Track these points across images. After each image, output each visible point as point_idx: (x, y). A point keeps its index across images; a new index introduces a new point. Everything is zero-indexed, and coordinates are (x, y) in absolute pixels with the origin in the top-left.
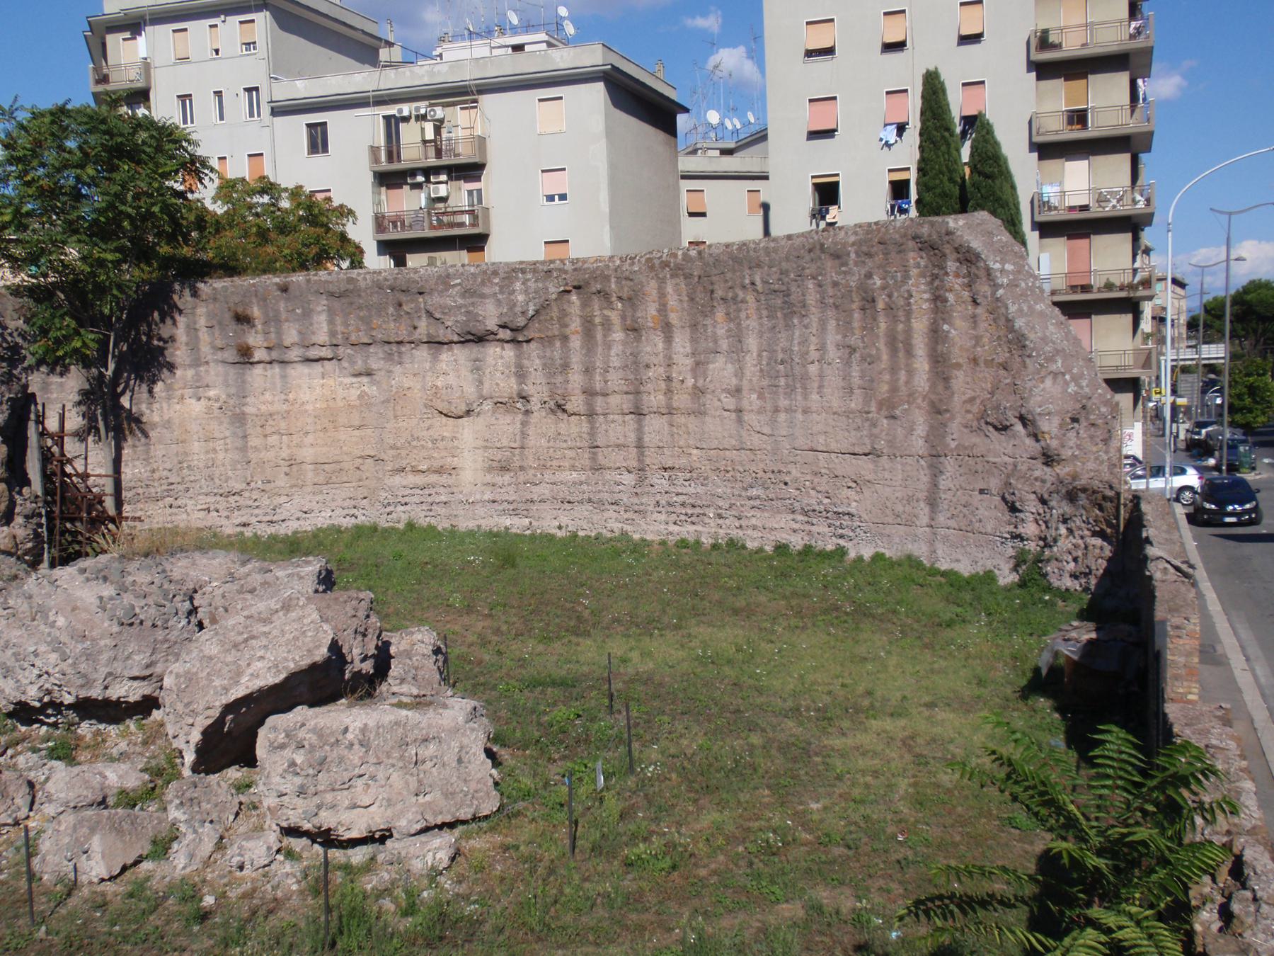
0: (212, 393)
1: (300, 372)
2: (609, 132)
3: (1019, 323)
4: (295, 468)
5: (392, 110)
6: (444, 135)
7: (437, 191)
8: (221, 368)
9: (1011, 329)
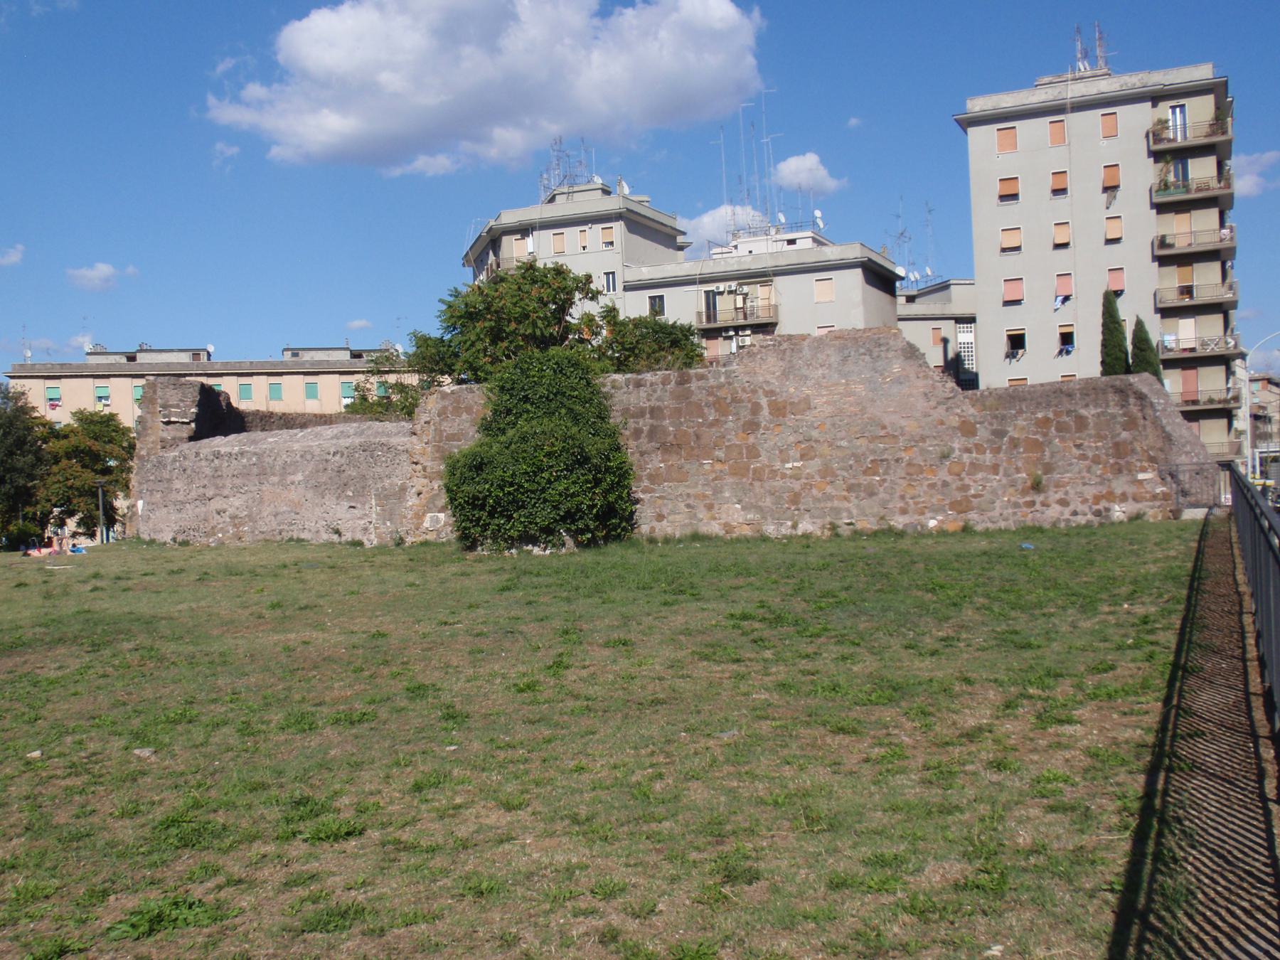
2: (865, 301)
3: (1168, 429)
5: (712, 287)
6: (749, 304)
7: (743, 341)
9: (1164, 431)
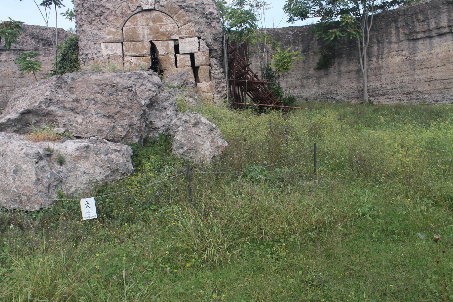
0: (404, 53)
1: (436, 41)
4: (432, 82)
8: (407, 43)
